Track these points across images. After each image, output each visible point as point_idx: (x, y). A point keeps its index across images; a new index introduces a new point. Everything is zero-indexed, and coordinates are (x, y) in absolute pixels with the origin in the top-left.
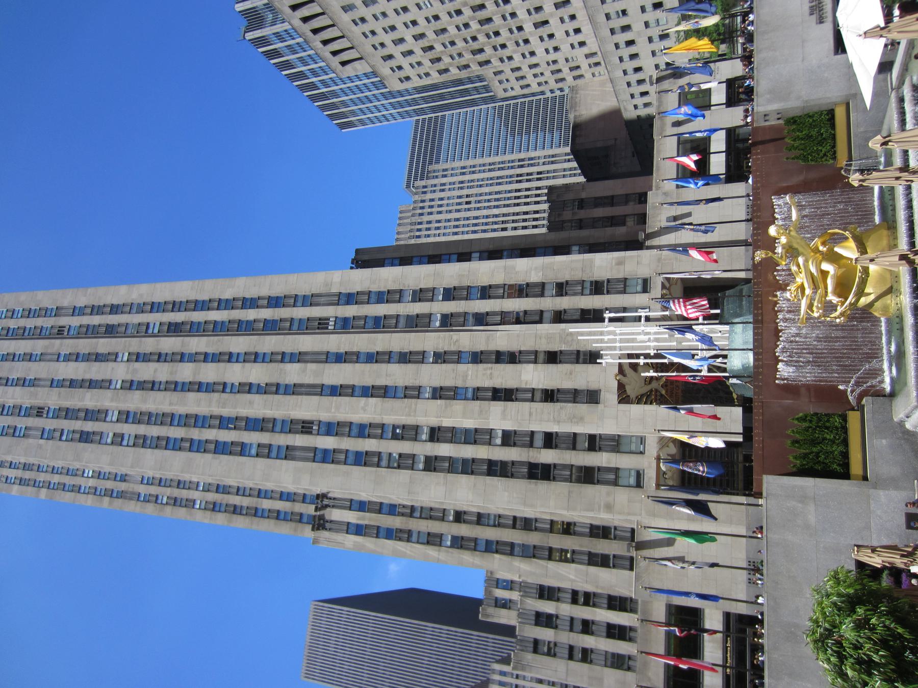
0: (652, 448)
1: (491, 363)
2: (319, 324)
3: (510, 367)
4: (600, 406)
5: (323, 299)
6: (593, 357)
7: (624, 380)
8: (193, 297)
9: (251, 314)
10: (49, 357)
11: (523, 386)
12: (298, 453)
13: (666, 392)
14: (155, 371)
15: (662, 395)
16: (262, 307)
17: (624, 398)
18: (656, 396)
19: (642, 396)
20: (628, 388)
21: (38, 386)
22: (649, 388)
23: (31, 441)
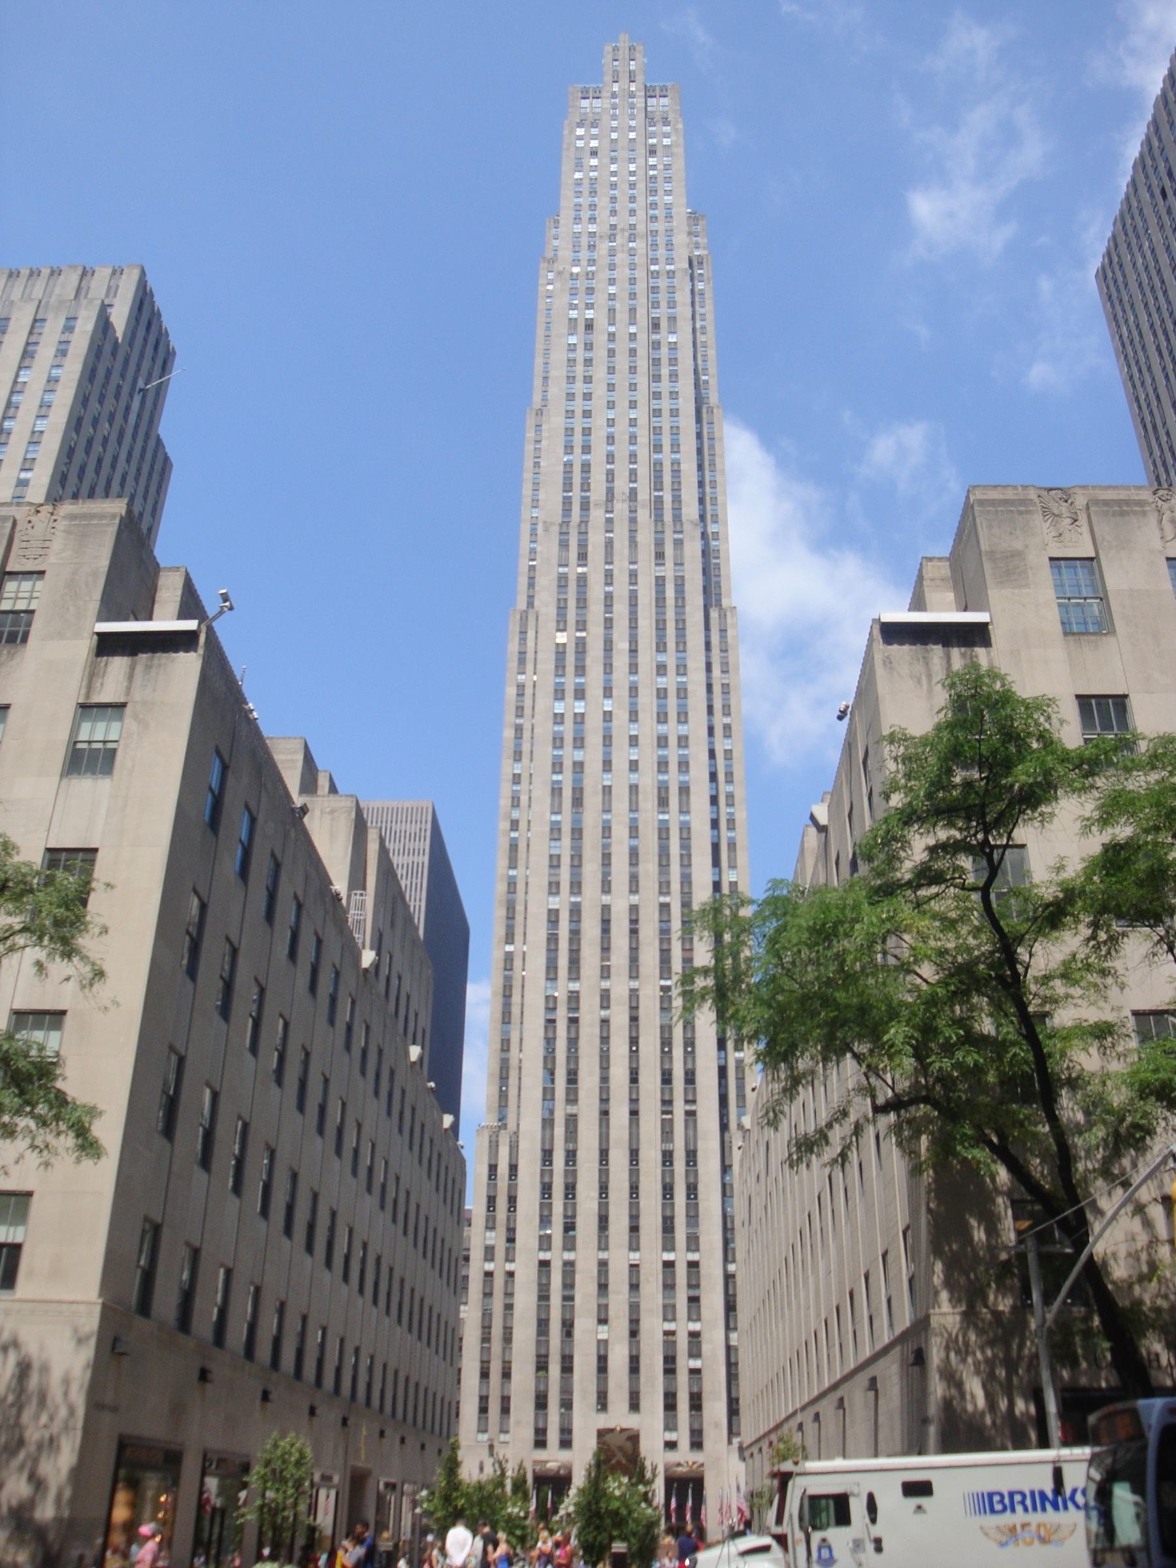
3: (626, 1333)
5: (691, 1133)
6: (635, 1406)
9: (678, 1052)
12: (548, 1132)
16: (685, 1063)
17: (601, 1433)
21: (604, 794)
23: (548, 800)
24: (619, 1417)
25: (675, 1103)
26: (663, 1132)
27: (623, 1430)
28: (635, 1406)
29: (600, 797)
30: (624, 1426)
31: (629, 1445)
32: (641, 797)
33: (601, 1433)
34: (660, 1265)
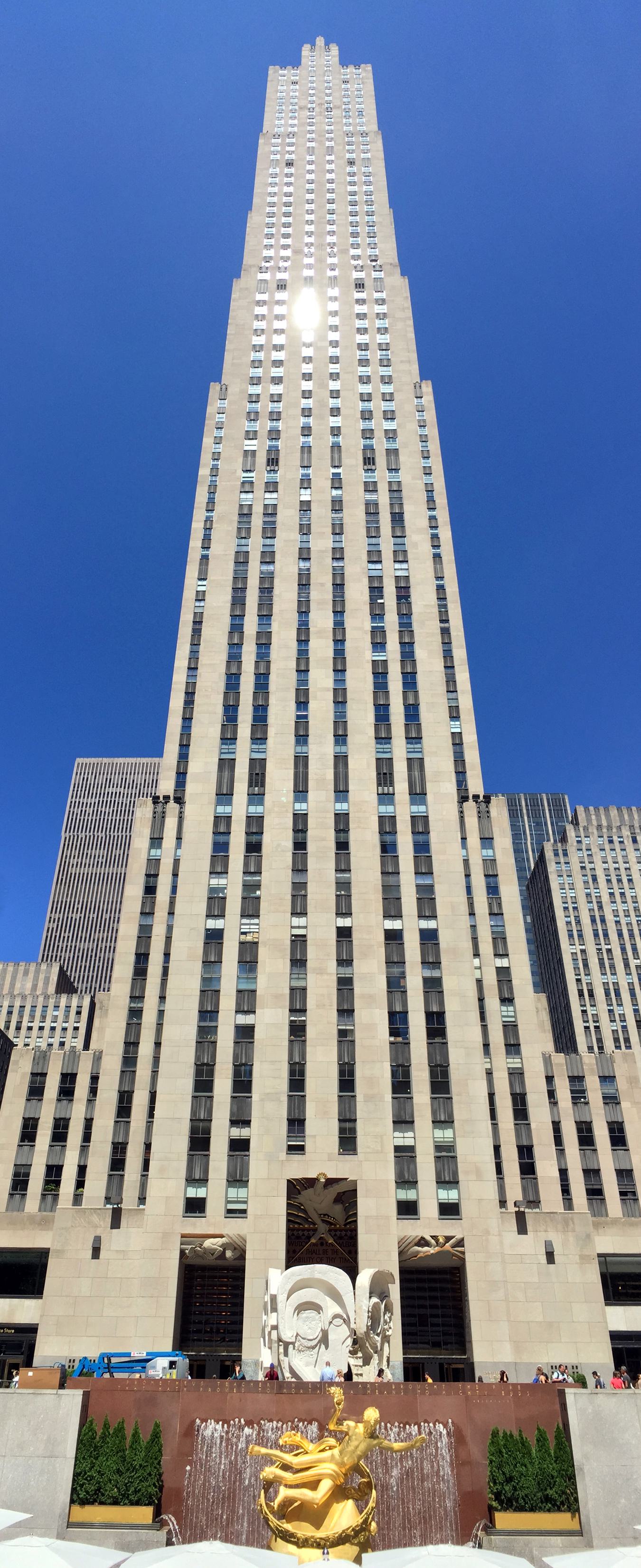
0: (233, 1228)
1: (339, 1004)
2: (385, 774)
4: (283, 1155)
5: (417, 773)
6: (348, 1141)
7: (319, 1187)
8: (416, 609)
10: (336, 456)
11: (308, 1049)
12: (226, 774)
13: (314, 1244)
14: (322, 585)
15: (309, 1238)
17: (295, 1188)
18: (308, 1230)
19: (305, 1211)
20: (310, 1191)
21: (302, 452)
22: (318, 1220)
24: (322, 1159)
25: (394, 741)
26: (378, 774)
27: (330, 1182)
28: (348, 1141)
29: (299, 454)
30: (331, 1175)
31: (337, 1212)
32: (343, 454)
33: (295, 1188)
34: (381, 937)
